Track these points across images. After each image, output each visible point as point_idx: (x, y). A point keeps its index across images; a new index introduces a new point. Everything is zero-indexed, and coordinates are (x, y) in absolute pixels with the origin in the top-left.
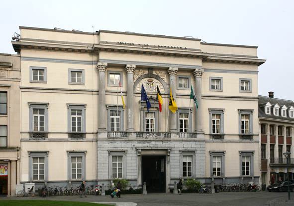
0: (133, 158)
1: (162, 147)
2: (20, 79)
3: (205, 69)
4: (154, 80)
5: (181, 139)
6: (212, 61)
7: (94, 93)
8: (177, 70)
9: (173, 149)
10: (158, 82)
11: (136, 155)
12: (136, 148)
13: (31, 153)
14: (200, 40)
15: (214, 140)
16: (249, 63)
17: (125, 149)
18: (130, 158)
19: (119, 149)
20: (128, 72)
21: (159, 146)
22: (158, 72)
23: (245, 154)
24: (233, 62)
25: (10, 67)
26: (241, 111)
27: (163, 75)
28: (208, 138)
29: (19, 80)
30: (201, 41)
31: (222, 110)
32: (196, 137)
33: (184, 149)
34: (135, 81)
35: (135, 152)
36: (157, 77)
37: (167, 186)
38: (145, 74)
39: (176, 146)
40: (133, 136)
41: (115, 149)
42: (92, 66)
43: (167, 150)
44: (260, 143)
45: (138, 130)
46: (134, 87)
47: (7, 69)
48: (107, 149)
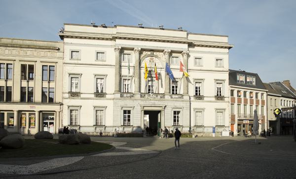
23: (219, 111)
35: (140, 108)
36: (156, 57)
39: (169, 104)
44: (230, 103)
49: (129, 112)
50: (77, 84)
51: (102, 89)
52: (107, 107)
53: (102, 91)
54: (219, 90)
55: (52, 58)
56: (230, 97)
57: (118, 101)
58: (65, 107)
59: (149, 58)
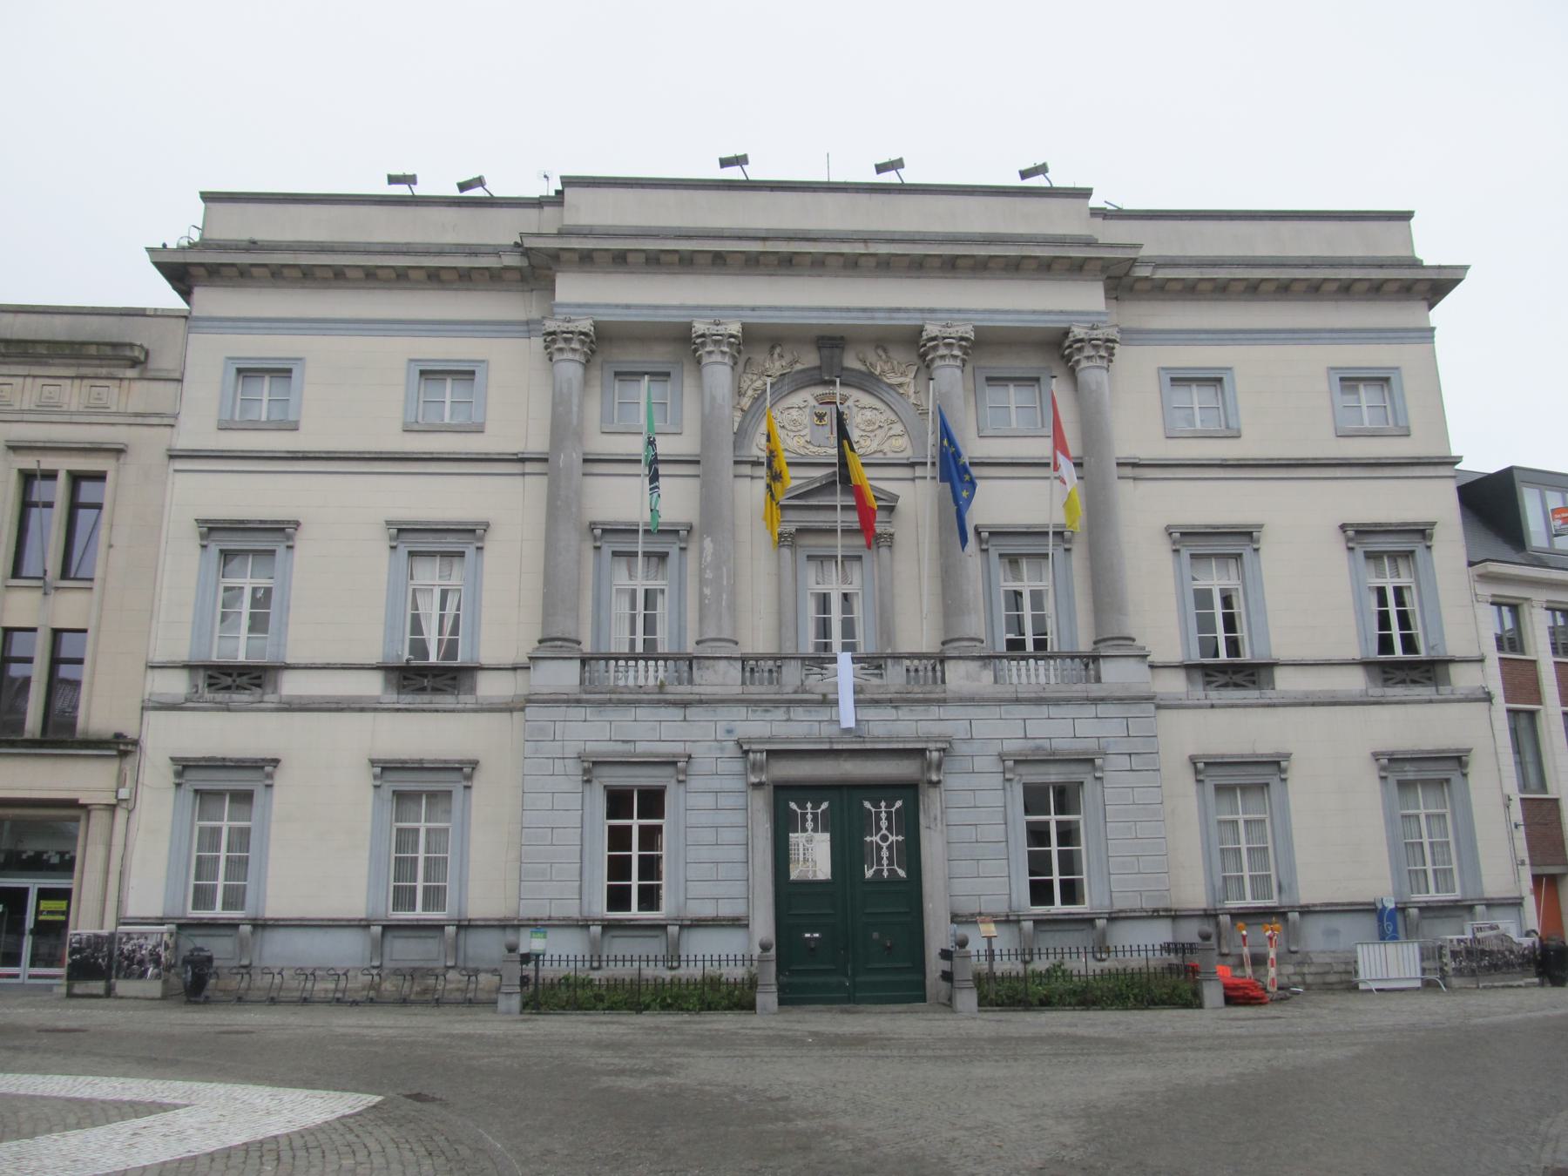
0: (725, 801)
1: (898, 739)
2: (176, 416)
3: (1122, 331)
4: (855, 394)
5: (1004, 691)
6: (1161, 290)
7: (529, 467)
8: (972, 335)
9: (961, 748)
10: (879, 405)
11: (739, 784)
12: (739, 743)
13: (184, 767)
14: (1086, 193)
15: (1215, 695)
16: (1376, 291)
17: (678, 748)
18: (708, 801)
19: (641, 747)
20: (705, 360)
21: (878, 730)
22: (871, 356)
23: (1410, 773)
24: (1285, 290)
25: (134, 363)
26: (1358, 533)
27: (897, 371)
28: (1174, 684)
29: (169, 421)
30: (1095, 202)
31: (1250, 534)
32: (1098, 679)
33: (1031, 744)
34: (746, 402)
35: (737, 766)
36: (867, 382)
37: (935, 966)
38: (798, 367)
39: (980, 729)
40: (723, 678)
41: (620, 747)
42: (527, 340)
43: (922, 752)
44: (1500, 705)
45: (758, 640)
46: (741, 436)
47: (119, 373)
48: (572, 749)
49: (653, 801)
50: (262, 599)
51: (455, 630)
52: (474, 764)
53: (451, 649)
54: (1392, 609)
55: (96, 414)
56: (1493, 656)
57: (559, 712)
58: (154, 768)
59: (807, 398)
